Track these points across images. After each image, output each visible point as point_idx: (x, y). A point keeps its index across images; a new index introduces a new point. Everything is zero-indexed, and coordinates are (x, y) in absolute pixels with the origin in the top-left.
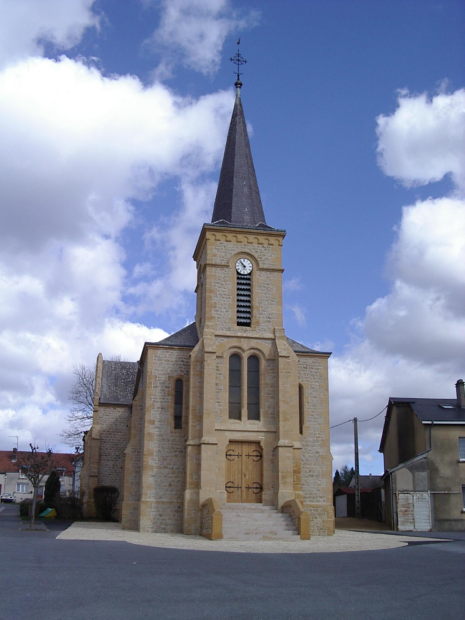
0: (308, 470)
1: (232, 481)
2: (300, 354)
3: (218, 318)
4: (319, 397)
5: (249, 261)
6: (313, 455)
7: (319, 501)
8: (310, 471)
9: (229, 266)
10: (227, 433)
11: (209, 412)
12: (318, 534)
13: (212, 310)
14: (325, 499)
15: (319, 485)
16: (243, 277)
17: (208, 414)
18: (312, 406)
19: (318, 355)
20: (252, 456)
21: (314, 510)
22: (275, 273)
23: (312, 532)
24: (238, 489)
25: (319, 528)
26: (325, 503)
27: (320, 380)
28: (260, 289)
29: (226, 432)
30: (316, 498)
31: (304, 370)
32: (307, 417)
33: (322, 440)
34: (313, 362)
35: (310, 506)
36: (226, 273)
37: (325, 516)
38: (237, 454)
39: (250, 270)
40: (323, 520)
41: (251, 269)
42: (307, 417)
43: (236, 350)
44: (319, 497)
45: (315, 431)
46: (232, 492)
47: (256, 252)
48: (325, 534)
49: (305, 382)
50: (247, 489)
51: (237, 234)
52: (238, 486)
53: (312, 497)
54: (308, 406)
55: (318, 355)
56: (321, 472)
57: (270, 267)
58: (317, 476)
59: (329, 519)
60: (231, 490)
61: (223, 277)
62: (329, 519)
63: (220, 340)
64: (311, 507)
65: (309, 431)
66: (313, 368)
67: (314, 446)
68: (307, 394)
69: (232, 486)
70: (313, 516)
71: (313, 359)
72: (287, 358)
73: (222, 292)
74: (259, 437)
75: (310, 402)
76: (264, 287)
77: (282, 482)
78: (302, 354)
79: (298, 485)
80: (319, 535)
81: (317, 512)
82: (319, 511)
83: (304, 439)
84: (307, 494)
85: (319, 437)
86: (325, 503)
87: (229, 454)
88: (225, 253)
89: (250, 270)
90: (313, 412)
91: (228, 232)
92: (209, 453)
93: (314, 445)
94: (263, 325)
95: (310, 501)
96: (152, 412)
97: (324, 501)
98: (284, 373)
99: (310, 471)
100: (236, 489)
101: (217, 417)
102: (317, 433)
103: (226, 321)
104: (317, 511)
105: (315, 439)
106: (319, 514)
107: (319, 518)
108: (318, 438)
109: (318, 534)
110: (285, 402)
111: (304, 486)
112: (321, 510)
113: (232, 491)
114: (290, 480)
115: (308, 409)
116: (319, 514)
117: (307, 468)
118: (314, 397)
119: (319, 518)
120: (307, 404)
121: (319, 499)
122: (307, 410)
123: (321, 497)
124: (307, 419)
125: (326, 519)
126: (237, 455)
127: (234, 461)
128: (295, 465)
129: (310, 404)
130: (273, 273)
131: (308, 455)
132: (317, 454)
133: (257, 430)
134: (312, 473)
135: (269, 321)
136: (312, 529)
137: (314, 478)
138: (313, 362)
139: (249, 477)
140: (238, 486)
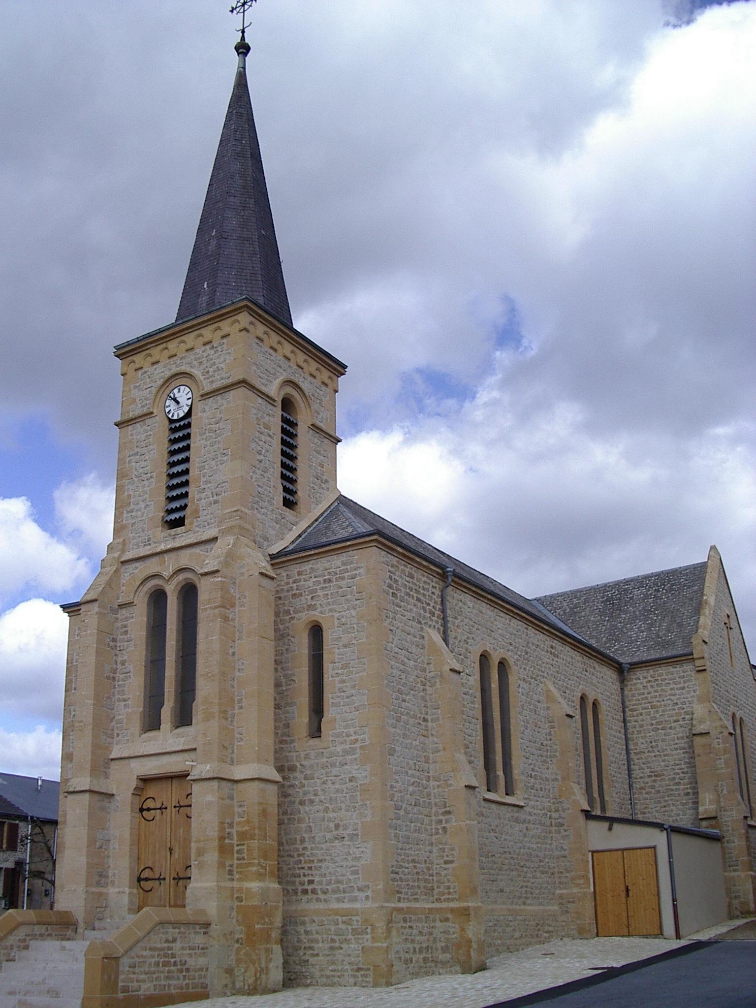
0: (332, 825)
1: (150, 866)
2: (313, 552)
3: (133, 524)
4: (356, 642)
5: (187, 388)
6: (344, 786)
7: (355, 899)
8: (337, 826)
9: (152, 413)
10: (134, 763)
11: (82, 724)
12: (352, 980)
13: (123, 513)
14: (369, 893)
15: (355, 859)
16: (177, 425)
17: (81, 731)
18: (342, 668)
19: (349, 543)
20: (186, 806)
21: (343, 922)
22: (232, 392)
23: (339, 977)
24: (160, 884)
25: (355, 967)
26: (369, 904)
27: (357, 602)
28: (203, 439)
29: (131, 760)
30: (349, 892)
31: (326, 587)
32: (330, 696)
33: (361, 747)
34: (344, 564)
35: (336, 912)
36: (149, 428)
37: (369, 936)
38: (159, 807)
39: (188, 405)
40: (363, 948)
41: (189, 402)
42: (330, 696)
43: (181, 577)
44: (356, 888)
45: (347, 726)
46: (151, 890)
47: (201, 362)
48: (367, 982)
49: (327, 615)
50: (177, 881)
51: (168, 343)
52: (160, 875)
53: (341, 889)
54: (333, 669)
55: (349, 543)
56: (359, 827)
57: (223, 383)
58: (353, 837)
59: (376, 945)
60: (147, 885)
61: (143, 439)
62: (376, 945)
63: (131, 569)
64: (337, 914)
65: (335, 729)
66: (343, 578)
67: (346, 764)
68: (330, 643)
69: (150, 877)
70: (340, 937)
71: (344, 557)
72: (216, 575)
73: (141, 471)
74: (187, 763)
75: (336, 661)
76: (211, 431)
77: (197, 862)
78: (316, 551)
79: (250, 868)
80: (355, 984)
81: (350, 927)
82: (355, 923)
83: (324, 751)
84: (331, 883)
85: (356, 740)
86: (369, 904)
87: (146, 808)
88: (150, 389)
89: (188, 405)
90: (344, 681)
91: (153, 345)
92: (78, 811)
93: (345, 761)
94: (205, 512)
95: (339, 900)
96: (71, 737)
97: (367, 897)
98: (209, 612)
99: (337, 826)
100: (158, 882)
101: (122, 732)
102: (352, 733)
103: (145, 526)
104: (349, 924)
105: (347, 747)
106: (355, 932)
107: (353, 941)
108: (355, 743)
109: (352, 980)
110: (209, 677)
111: (324, 865)
112: (358, 921)
113: (150, 889)
114: (212, 857)
115: (332, 676)
116: (355, 932)
117: (330, 820)
118: (345, 646)
119: (353, 941)
120: (331, 665)
121: (356, 893)
122: (330, 679)
123: (360, 889)
124: (331, 701)
125: (369, 944)
126: (160, 809)
127: (154, 821)
128: (245, 819)
129: (337, 664)
130: (226, 395)
131: (332, 787)
132: (352, 784)
133: (180, 748)
134: (341, 832)
135: (216, 502)
136: (340, 968)
137: (346, 842)
138: (344, 564)
139: (179, 855)
140: (160, 875)
